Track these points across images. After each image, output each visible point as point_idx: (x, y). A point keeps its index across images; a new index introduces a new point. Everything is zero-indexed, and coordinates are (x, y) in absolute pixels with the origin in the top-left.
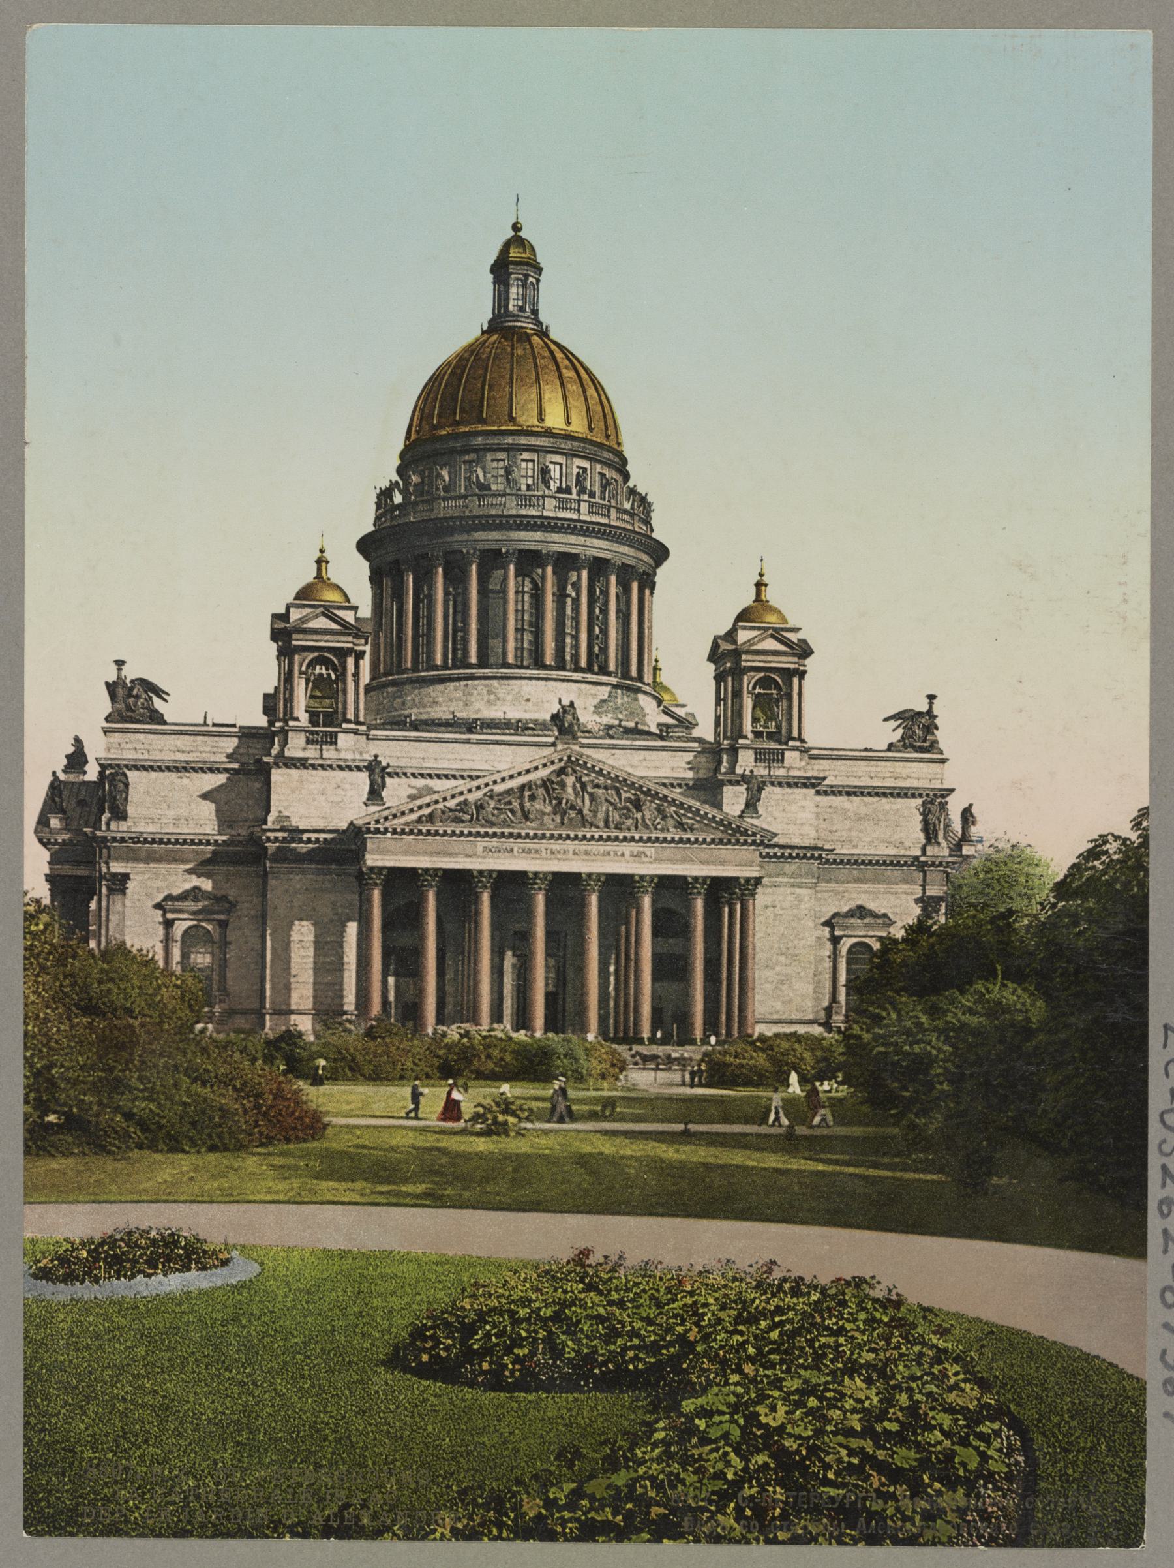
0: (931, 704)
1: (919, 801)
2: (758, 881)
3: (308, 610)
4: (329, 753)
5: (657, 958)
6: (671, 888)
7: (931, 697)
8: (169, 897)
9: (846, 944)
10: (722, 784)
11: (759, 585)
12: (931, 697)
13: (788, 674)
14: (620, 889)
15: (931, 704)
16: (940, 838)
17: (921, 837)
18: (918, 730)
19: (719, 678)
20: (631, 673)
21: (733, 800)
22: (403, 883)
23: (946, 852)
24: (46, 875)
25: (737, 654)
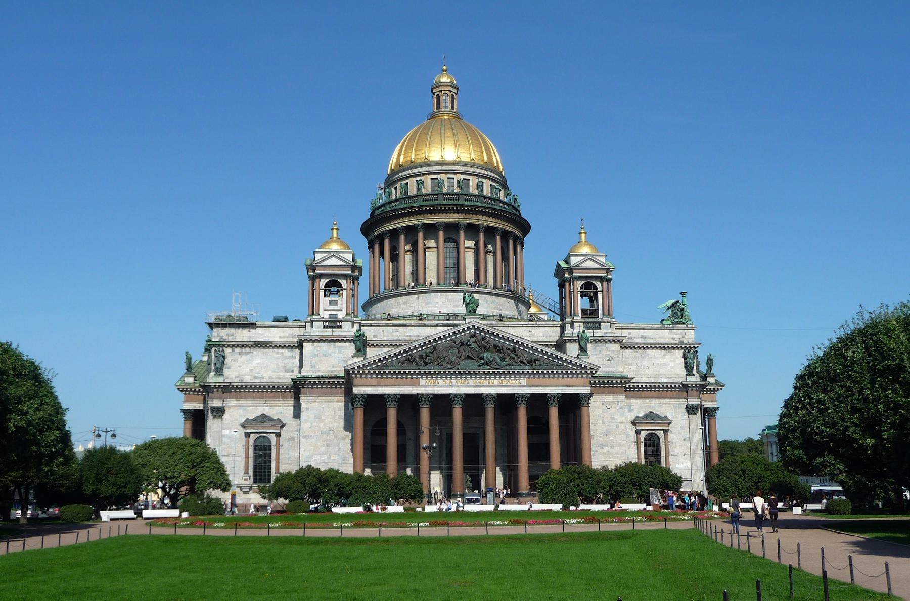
1: (682, 351)
2: (590, 396)
3: (324, 255)
4: (337, 332)
5: (530, 446)
6: (538, 404)
7: (683, 294)
8: (247, 420)
9: (643, 434)
10: (566, 342)
13: (601, 279)
14: (507, 403)
17: (683, 372)
19: (561, 286)
21: (572, 350)
22: (375, 404)
23: (699, 380)
24: (184, 411)
25: (571, 270)
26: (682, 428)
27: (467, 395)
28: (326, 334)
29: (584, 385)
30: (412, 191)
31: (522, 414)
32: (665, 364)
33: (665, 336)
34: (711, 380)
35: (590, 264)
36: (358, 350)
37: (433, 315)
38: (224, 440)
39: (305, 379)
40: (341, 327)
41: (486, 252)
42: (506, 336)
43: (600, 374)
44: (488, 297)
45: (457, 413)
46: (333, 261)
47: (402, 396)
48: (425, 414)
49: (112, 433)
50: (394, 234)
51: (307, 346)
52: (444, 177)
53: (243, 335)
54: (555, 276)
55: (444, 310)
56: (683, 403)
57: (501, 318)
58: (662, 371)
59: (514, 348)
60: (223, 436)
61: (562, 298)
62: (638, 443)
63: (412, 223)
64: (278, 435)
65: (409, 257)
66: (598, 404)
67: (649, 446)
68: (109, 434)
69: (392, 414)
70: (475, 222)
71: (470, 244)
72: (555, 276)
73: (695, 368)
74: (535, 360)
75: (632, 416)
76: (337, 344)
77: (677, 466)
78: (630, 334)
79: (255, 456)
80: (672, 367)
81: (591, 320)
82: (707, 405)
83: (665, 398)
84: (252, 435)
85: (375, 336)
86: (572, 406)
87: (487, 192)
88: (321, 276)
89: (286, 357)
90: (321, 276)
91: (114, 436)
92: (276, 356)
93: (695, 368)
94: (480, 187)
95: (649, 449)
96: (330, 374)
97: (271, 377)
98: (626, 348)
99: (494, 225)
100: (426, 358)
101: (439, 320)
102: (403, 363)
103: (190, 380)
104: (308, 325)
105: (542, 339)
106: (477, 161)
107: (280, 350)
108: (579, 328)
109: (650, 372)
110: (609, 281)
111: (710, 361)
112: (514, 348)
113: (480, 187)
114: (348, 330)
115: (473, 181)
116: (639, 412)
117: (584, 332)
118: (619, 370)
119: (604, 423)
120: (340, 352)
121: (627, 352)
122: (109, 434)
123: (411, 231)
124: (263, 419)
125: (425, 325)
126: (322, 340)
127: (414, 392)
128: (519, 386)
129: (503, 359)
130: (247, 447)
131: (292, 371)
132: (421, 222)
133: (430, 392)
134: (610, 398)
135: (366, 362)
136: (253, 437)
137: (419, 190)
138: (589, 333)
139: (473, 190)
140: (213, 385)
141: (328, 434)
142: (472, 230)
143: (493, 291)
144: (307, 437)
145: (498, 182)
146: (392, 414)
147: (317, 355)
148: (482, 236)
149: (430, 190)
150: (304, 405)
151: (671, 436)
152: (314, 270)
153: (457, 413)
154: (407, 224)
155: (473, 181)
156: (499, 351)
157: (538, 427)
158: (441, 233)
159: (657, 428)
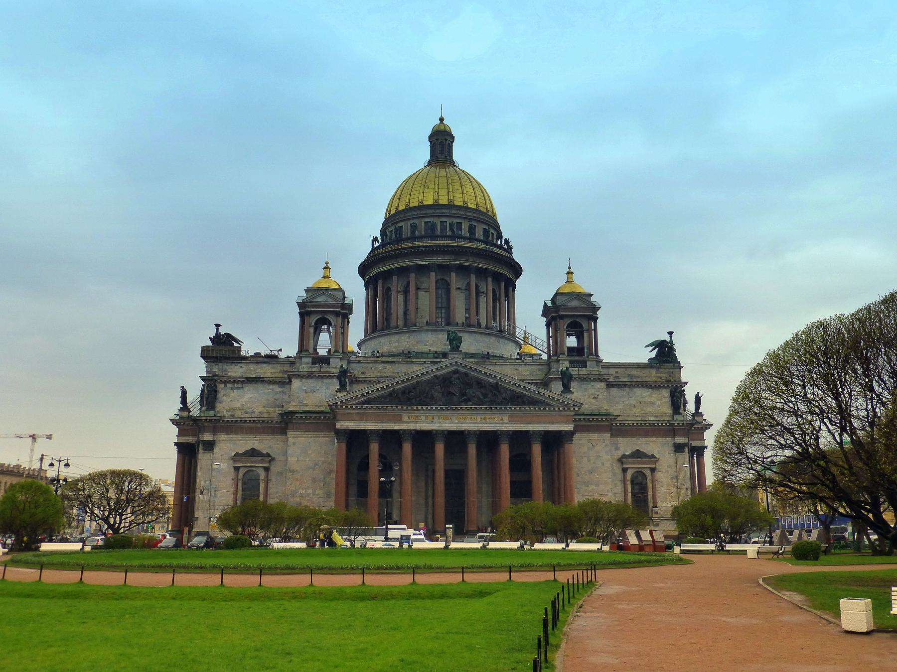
0: (671, 337)
1: (668, 390)
4: (325, 368)
6: (520, 439)
7: (671, 333)
8: (237, 455)
10: (551, 380)
11: (569, 273)
12: (671, 333)
14: (489, 441)
15: (671, 337)
16: (682, 411)
18: (665, 352)
19: (548, 325)
20: (506, 332)
24: (176, 444)
26: (670, 466)
27: (451, 433)
28: (314, 370)
29: (567, 422)
30: (406, 233)
31: (505, 450)
32: (653, 403)
33: (652, 375)
34: (698, 419)
35: (575, 303)
36: (343, 387)
37: (422, 353)
38: (214, 473)
39: (292, 413)
40: (329, 364)
41: (478, 292)
42: (488, 372)
43: (581, 411)
44: (478, 337)
45: (440, 449)
46: (321, 299)
47: (385, 431)
48: (407, 448)
49: (65, 462)
50: (387, 275)
51: (296, 384)
52: (437, 221)
53: (235, 371)
54: (543, 315)
55: (433, 349)
56: (669, 440)
57: (487, 356)
58: (649, 409)
59: (497, 384)
60: (212, 470)
61: (549, 337)
62: (624, 481)
63: (405, 264)
64: (267, 469)
65: (401, 298)
66: (583, 441)
67: (637, 484)
68: (62, 464)
69: (374, 448)
70: (467, 264)
71: (462, 284)
72: (543, 315)
73: (682, 407)
74: (518, 397)
75: (619, 454)
76: (325, 381)
77: (665, 504)
78: (617, 372)
79: (243, 490)
80: (659, 406)
81: (576, 358)
82: (695, 443)
83: (652, 436)
84: (241, 470)
85: (363, 373)
86: (554, 443)
87: (479, 233)
88: (309, 313)
89: (276, 393)
90: (309, 313)
91: (67, 465)
92: (266, 391)
93: (682, 407)
94: (472, 229)
95: (636, 487)
96: (317, 409)
97: (260, 413)
98: (613, 386)
99: (485, 266)
100: (411, 395)
101: (427, 358)
102: (386, 398)
103: (185, 414)
104: (298, 364)
105: (528, 377)
106: (470, 205)
107: (271, 386)
108: (565, 365)
109: (637, 411)
110: (595, 319)
111: (698, 400)
112: (497, 384)
113: (472, 229)
114: (335, 365)
115: (465, 226)
116: (626, 451)
117: (567, 368)
118: (604, 406)
119: (589, 460)
120: (327, 388)
121: (614, 391)
122: (62, 464)
123: (403, 271)
124: (253, 453)
125: (412, 362)
126: (310, 376)
127: (397, 428)
128: (500, 422)
129: (485, 396)
130: (236, 480)
131: (283, 406)
132: (413, 263)
133: (412, 428)
134: (595, 436)
135: (348, 397)
136: (242, 472)
137: (413, 232)
138: (574, 371)
139: (465, 232)
140: (204, 418)
141: (314, 469)
142: (463, 270)
143: (482, 331)
144: (293, 472)
145: (489, 225)
146: (374, 448)
147: (305, 391)
148: (473, 277)
149: (423, 233)
150: (291, 440)
151: (659, 475)
152: (304, 308)
153: (440, 449)
154: (400, 265)
155: (465, 226)
156: (481, 387)
157: (521, 463)
158: (433, 274)
159: (645, 467)
